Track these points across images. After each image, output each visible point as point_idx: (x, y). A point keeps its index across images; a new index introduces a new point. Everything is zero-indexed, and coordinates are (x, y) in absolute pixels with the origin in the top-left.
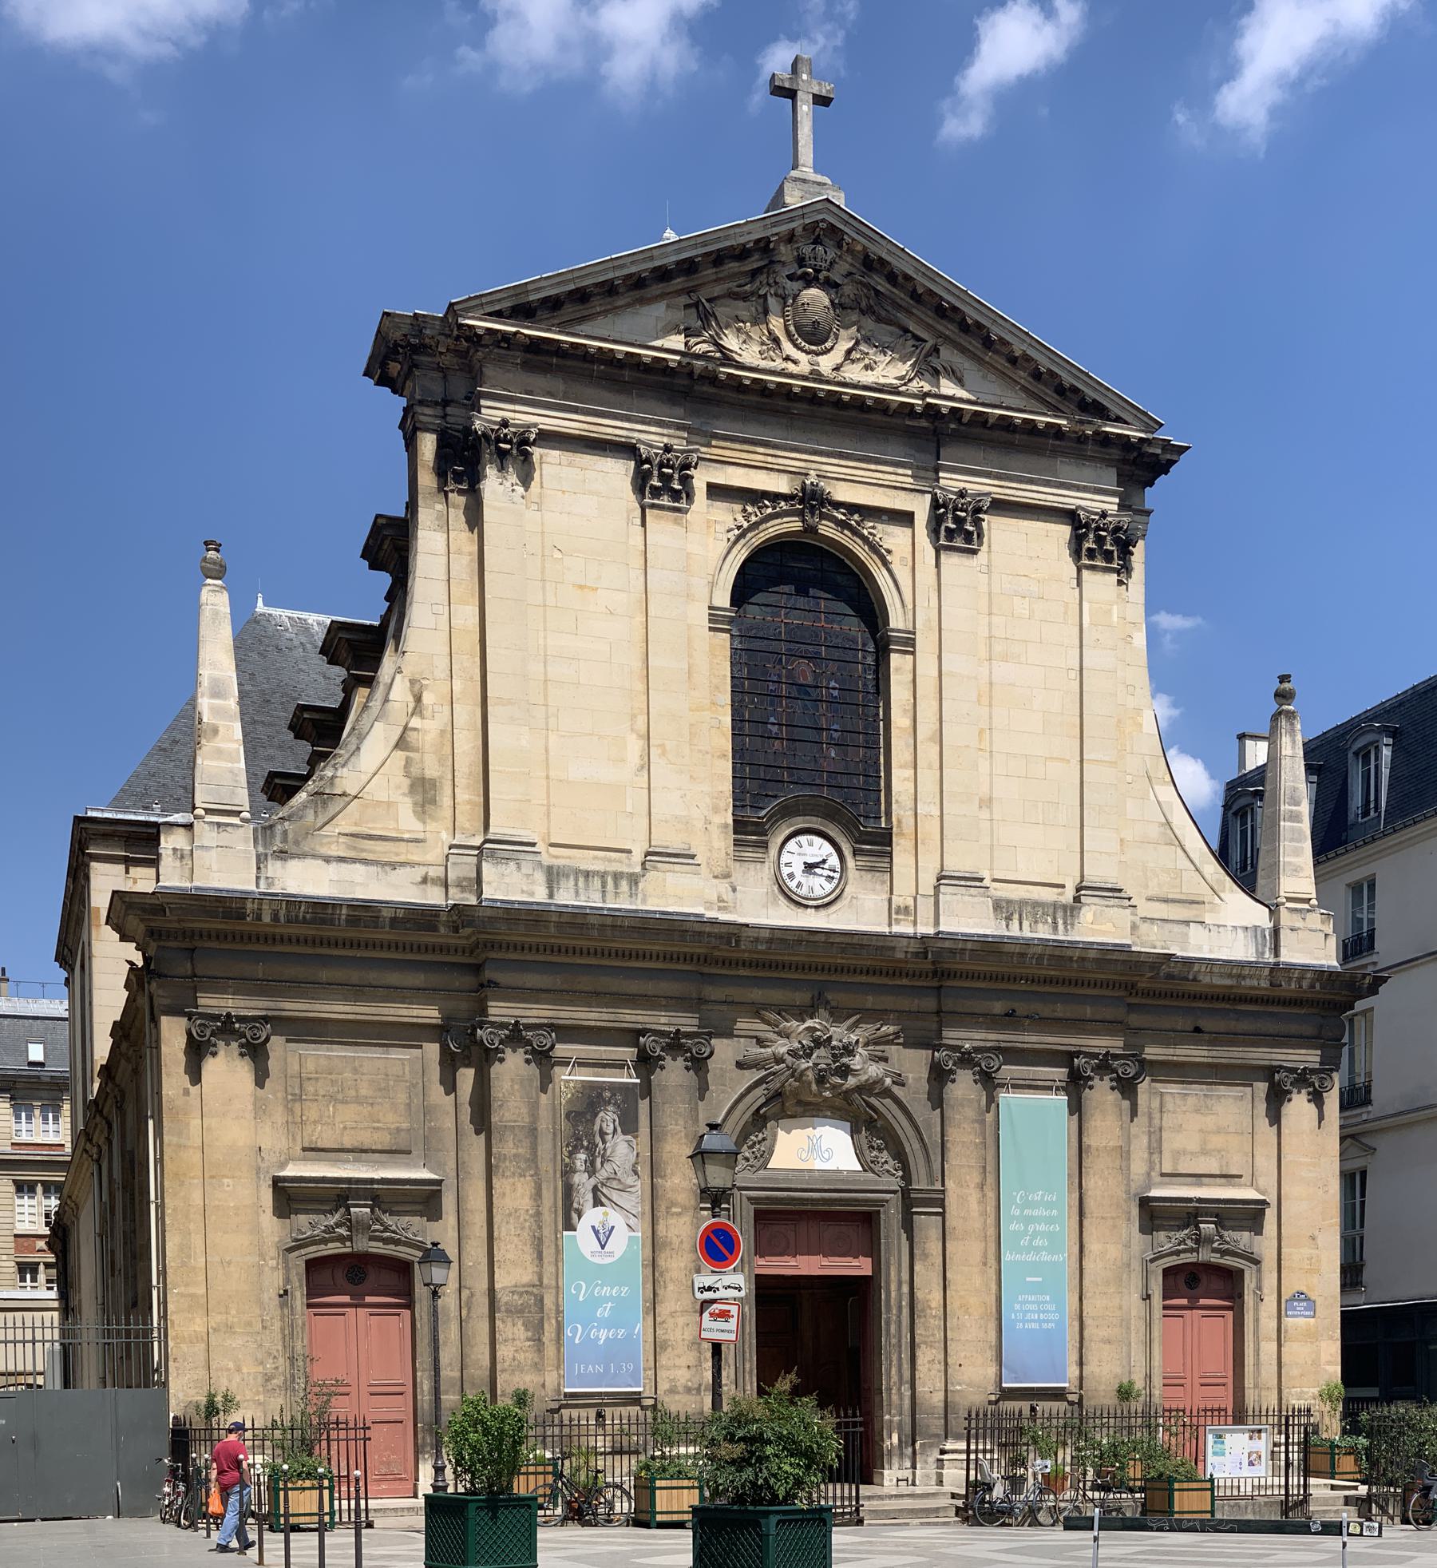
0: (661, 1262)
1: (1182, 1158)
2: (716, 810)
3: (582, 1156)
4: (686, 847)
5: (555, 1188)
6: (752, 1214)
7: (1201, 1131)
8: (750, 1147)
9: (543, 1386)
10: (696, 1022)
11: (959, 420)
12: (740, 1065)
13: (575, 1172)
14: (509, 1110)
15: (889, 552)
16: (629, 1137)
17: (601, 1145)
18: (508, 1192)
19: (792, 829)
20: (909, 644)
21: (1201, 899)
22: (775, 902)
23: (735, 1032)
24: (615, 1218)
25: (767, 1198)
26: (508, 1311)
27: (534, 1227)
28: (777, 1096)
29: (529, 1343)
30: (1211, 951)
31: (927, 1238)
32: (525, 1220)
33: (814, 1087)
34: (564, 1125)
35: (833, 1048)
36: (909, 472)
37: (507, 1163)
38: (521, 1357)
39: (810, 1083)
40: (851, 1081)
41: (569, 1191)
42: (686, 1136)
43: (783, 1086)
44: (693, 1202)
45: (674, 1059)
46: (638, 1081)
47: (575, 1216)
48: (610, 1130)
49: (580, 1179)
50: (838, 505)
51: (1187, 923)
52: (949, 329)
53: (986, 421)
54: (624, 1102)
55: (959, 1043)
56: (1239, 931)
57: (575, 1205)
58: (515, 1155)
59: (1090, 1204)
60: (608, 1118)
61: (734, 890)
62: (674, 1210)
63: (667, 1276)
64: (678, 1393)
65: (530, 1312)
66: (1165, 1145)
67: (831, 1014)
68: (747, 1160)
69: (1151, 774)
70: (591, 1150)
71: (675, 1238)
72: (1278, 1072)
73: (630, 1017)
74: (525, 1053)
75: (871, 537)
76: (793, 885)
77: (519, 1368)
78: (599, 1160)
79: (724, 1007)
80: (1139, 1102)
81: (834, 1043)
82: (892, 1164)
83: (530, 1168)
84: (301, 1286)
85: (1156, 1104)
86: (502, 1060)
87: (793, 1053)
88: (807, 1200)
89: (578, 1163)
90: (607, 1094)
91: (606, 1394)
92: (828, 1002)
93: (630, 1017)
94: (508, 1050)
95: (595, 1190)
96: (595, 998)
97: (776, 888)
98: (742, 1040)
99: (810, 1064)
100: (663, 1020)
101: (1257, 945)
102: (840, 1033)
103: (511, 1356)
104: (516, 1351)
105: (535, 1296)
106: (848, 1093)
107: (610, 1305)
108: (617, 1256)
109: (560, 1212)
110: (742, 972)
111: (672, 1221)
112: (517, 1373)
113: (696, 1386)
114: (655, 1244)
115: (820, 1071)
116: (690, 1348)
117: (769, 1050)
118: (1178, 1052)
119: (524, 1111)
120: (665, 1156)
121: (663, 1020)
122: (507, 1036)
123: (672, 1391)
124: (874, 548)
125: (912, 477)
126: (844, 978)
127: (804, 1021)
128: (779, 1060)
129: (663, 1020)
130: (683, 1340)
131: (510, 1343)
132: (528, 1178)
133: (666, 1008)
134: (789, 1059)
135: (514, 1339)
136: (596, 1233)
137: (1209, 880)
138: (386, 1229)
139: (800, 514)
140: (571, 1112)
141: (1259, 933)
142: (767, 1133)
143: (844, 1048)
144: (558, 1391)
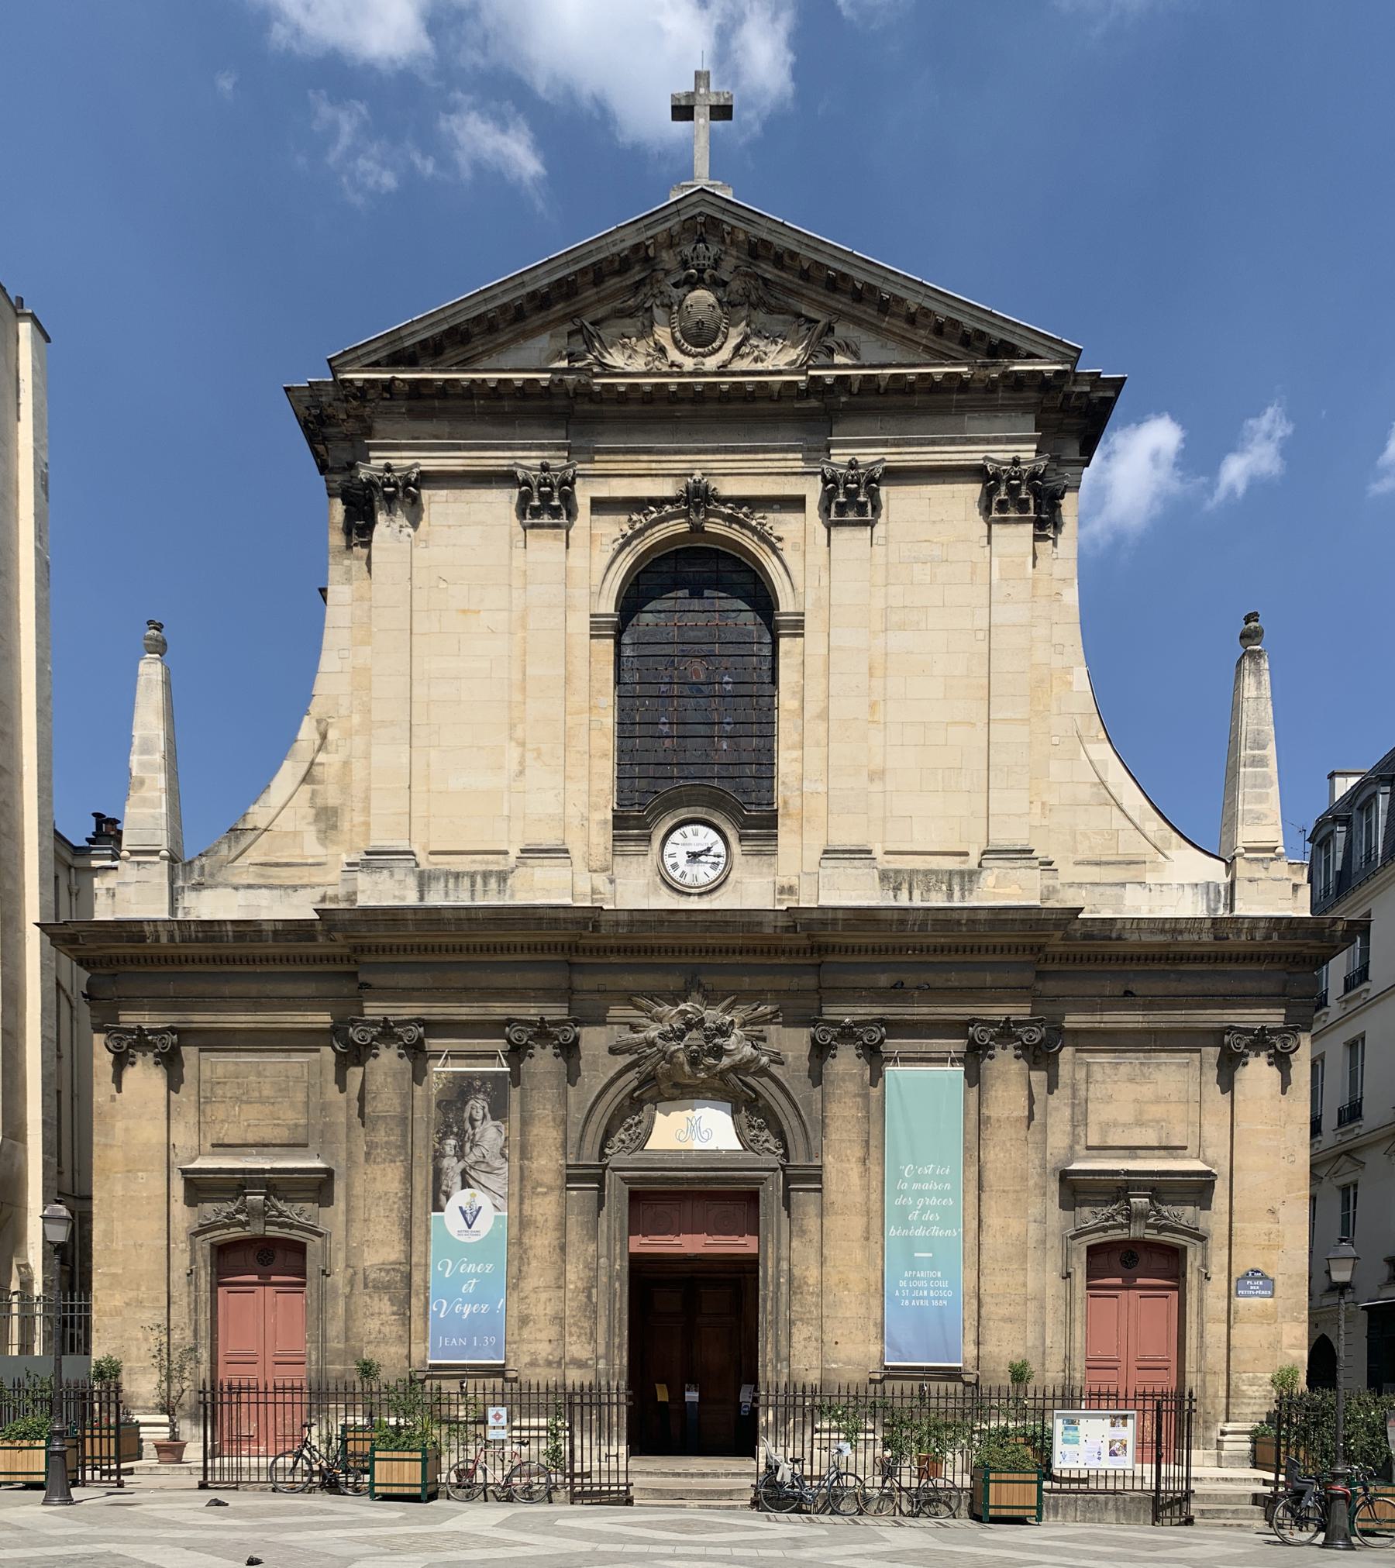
0: (526, 1240)
1: (1113, 1130)
2: (593, 807)
3: (451, 1142)
4: (559, 842)
5: (427, 1172)
6: (627, 1194)
7: (1136, 1101)
8: (626, 1130)
9: (409, 1357)
10: (565, 1010)
12: (613, 1051)
13: (444, 1157)
16: (498, 1123)
17: (470, 1131)
18: (379, 1177)
19: (676, 820)
20: (797, 627)
21: (1142, 859)
22: (656, 890)
23: (608, 1020)
24: (483, 1199)
25: (641, 1178)
26: (374, 1287)
28: (648, 1080)
29: (394, 1317)
30: (1150, 911)
31: (805, 1215)
32: (394, 1203)
33: (687, 1068)
34: (434, 1112)
35: (705, 1029)
36: (800, 456)
38: (386, 1330)
39: (682, 1065)
40: (726, 1061)
41: (438, 1174)
42: (554, 1119)
43: (654, 1069)
44: (559, 1182)
45: (543, 1048)
46: (508, 1069)
47: (443, 1198)
48: (479, 1116)
49: (450, 1163)
51: (1123, 884)
54: (493, 1089)
55: (839, 1018)
56: (1188, 890)
57: (444, 1188)
58: (386, 1142)
59: (990, 1177)
60: (478, 1106)
61: (612, 881)
62: (539, 1190)
63: (531, 1253)
64: (539, 1366)
65: (396, 1288)
66: (1092, 1118)
67: (705, 997)
68: (623, 1141)
69: (1082, 733)
70: (461, 1136)
72: (1228, 1034)
73: (499, 1009)
74: (399, 1048)
75: (759, 527)
76: (676, 874)
77: (383, 1340)
78: (468, 1145)
79: (597, 997)
80: (1061, 1072)
81: (707, 1025)
82: (773, 1143)
83: (400, 1154)
84: (205, 1266)
85: (1081, 1074)
86: (376, 1056)
87: (663, 1036)
88: (682, 1179)
89: (448, 1148)
90: (478, 1083)
91: (469, 1366)
92: (700, 985)
93: (499, 1009)
94: (382, 1047)
95: (464, 1173)
96: (465, 994)
98: (616, 1027)
99: (682, 1046)
100: (532, 1011)
101: (1208, 900)
102: (713, 1015)
104: (382, 1324)
105: (402, 1273)
106: (723, 1074)
107: (474, 1281)
108: (483, 1234)
109: (430, 1194)
110: (614, 959)
113: (557, 1359)
114: (524, 1223)
115: (691, 1052)
116: (552, 1323)
117: (642, 1035)
118: (1106, 1018)
119: (396, 1101)
120: (532, 1139)
121: (531, 1011)
122: (380, 1034)
123: (533, 1364)
124: (764, 538)
125: (802, 460)
126: (719, 960)
127: (678, 1006)
128: (651, 1044)
129: (531, 1011)
130: (545, 1315)
132: (398, 1164)
133: (536, 999)
134: (660, 1042)
135: (380, 1314)
136: (464, 1213)
137: (1153, 840)
138: (281, 1214)
140: (442, 1101)
141: (1212, 888)
142: (643, 1115)
143: (717, 1029)
144: (424, 1363)
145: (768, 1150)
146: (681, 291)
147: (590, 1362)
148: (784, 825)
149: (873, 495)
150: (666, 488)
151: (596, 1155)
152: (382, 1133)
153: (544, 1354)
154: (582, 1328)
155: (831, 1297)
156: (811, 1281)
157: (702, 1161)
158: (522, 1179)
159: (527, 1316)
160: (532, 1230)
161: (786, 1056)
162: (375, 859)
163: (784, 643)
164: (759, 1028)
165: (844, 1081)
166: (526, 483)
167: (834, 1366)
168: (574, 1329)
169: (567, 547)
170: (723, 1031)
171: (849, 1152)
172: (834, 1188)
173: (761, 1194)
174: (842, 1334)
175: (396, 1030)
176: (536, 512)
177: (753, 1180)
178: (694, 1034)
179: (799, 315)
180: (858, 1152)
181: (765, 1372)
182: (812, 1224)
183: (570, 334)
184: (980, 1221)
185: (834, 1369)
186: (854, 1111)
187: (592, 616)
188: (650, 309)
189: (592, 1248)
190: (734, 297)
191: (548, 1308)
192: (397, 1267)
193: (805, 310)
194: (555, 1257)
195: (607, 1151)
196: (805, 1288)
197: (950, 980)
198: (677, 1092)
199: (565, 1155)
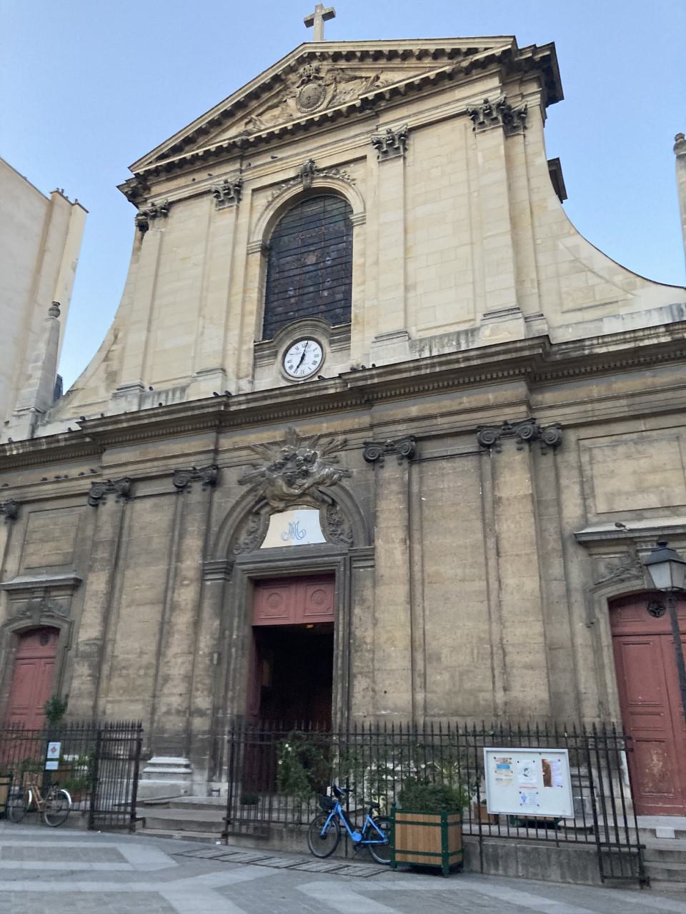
0: (173, 620)
6: (245, 581)
9: (95, 707)
12: (241, 483)
15: (353, 180)
20: (363, 221)
25: (256, 569)
29: (89, 678)
38: (83, 687)
43: (264, 492)
50: (324, 169)
52: (382, 63)
58: (102, 558)
62: (186, 582)
63: (175, 628)
77: (80, 695)
87: (269, 469)
97: (280, 377)
98: (243, 467)
104: (82, 683)
111: (183, 590)
119: (111, 530)
120: (184, 547)
123: (168, 713)
128: (263, 475)
130: (179, 674)
134: (267, 472)
139: (301, 182)
145: (342, 540)
146: (300, 89)
148: (354, 329)
149: (404, 143)
150: (292, 174)
151: (225, 554)
153: (175, 706)
154: (204, 684)
155: (382, 652)
156: (369, 640)
158: (176, 575)
159: (169, 675)
160: (178, 612)
161: (352, 472)
162: (121, 392)
163: (356, 230)
164: (335, 454)
165: (389, 483)
166: (217, 191)
167: (383, 712)
168: (200, 686)
169: (237, 214)
170: (309, 460)
171: (393, 535)
172: (383, 564)
173: (337, 574)
174: (390, 685)
176: (222, 202)
177: (332, 564)
178: (289, 465)
179: (361, 78)
180: (401, 534)
181: (336, 718)
182: (368, 593)
183: (247, 124)
184: (500, 582)
185: (384, 715)
186: (397, 505)
188: (286, 101)
189: (217, 623)
190: (327, 83)
193: (364, 74)
194: (190, 631)
195: (236, 552)
196: (365, 646)
197: (462, 403)
198: (282, 505)
199: (204, 556)
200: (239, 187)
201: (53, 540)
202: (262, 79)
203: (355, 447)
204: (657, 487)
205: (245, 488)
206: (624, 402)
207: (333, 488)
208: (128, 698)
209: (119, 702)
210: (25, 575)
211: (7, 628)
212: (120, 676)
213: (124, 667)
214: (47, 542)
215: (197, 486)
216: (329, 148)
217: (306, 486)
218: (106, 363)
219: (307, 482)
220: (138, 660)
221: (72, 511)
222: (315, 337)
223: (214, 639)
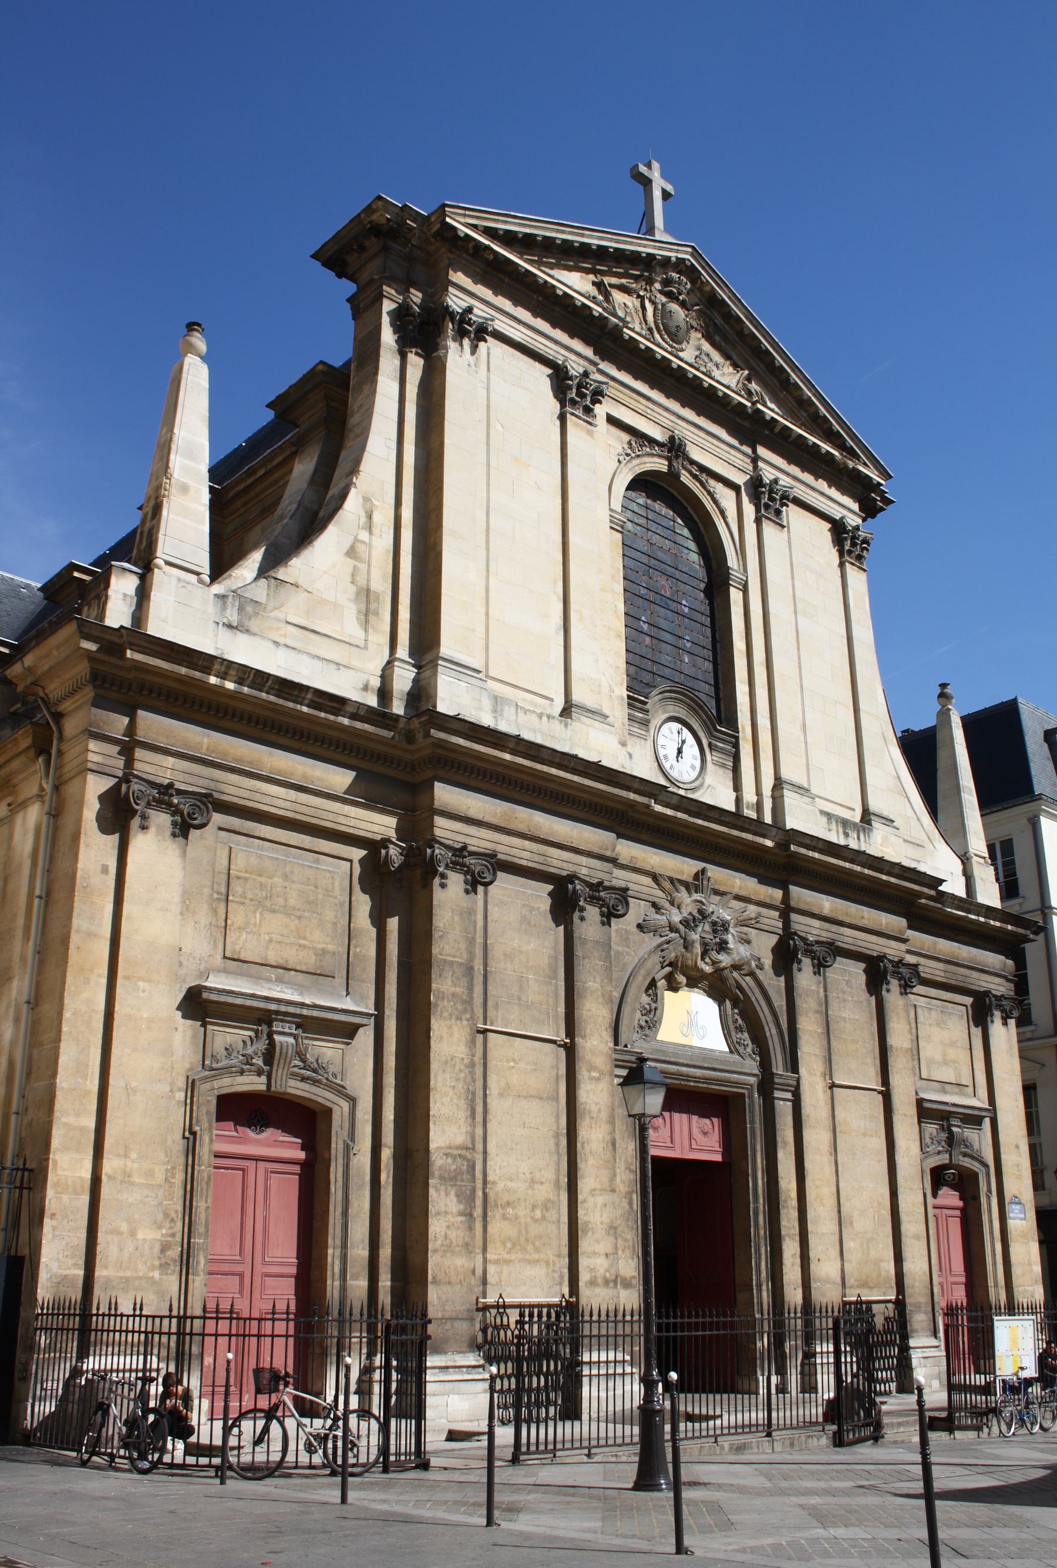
11: (772, 429)
14: (448, 943)
26: (441, 1177)
27: (469, 1079)
29: (463, 1218)
32: (461, 1071)
37: (446, 1003)
38: (453, 1234)
42: (603, 995)
44: (609, 1068)
53: (790, 436)
58: (453, 995)
64: (598, 1285)
65: (462, 1180)
71: (593, 1106)
77: (448, 1248)
83: (465, 1011)
87: (685, 922)
103: (443, 1233)
104: (448, 1227)
105: (468, 1160)
112: (448, 1255)
113: (613, 1277)
116: (608, 1233)
119: (463, 946)
123: (593, 1283)
128: (672, 929)
131: (442, 1218)
132: (465, 1022)
134: (682, 928)
135: (446, 1213)
147: (634, 1282)
152: (450, 983)
153: (602, 1271)
154: (626, 1240)
157: (704, 1059)
164: (745, 929)
175: (467, 860)
177: (737, 1084)
186: (815, 1026)
187: (611, 510)
191: (604, 1215)
192: (463, 1152)
194: (609, 1155)
200: (598, 395)
201: (288, 911)
202: (640, 245)
203: (766, 928)
204: (954, 1062)
205: (651, 941)
206: (941, 965)
207: (748, 979)
208: (520, 1255)
209: (508, 1262)
210: (225, 971)
211: (205, 1087)
212: (504, 1217)
213: (508, 1203)
214: (274, 911)
215: (593, 913)
216: (702, 434)
217: (723, 965)
218: (351, 562)
219: (725, 960)
220: (530, 1192)
221: (317, 861)
222: (696, 726)
223: (631, 1170)
